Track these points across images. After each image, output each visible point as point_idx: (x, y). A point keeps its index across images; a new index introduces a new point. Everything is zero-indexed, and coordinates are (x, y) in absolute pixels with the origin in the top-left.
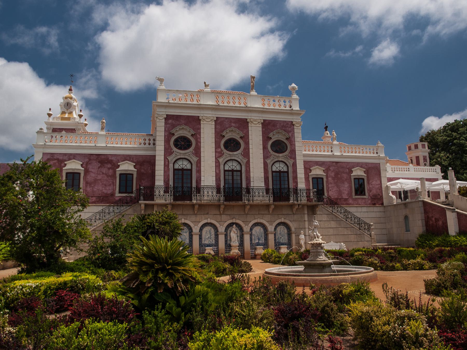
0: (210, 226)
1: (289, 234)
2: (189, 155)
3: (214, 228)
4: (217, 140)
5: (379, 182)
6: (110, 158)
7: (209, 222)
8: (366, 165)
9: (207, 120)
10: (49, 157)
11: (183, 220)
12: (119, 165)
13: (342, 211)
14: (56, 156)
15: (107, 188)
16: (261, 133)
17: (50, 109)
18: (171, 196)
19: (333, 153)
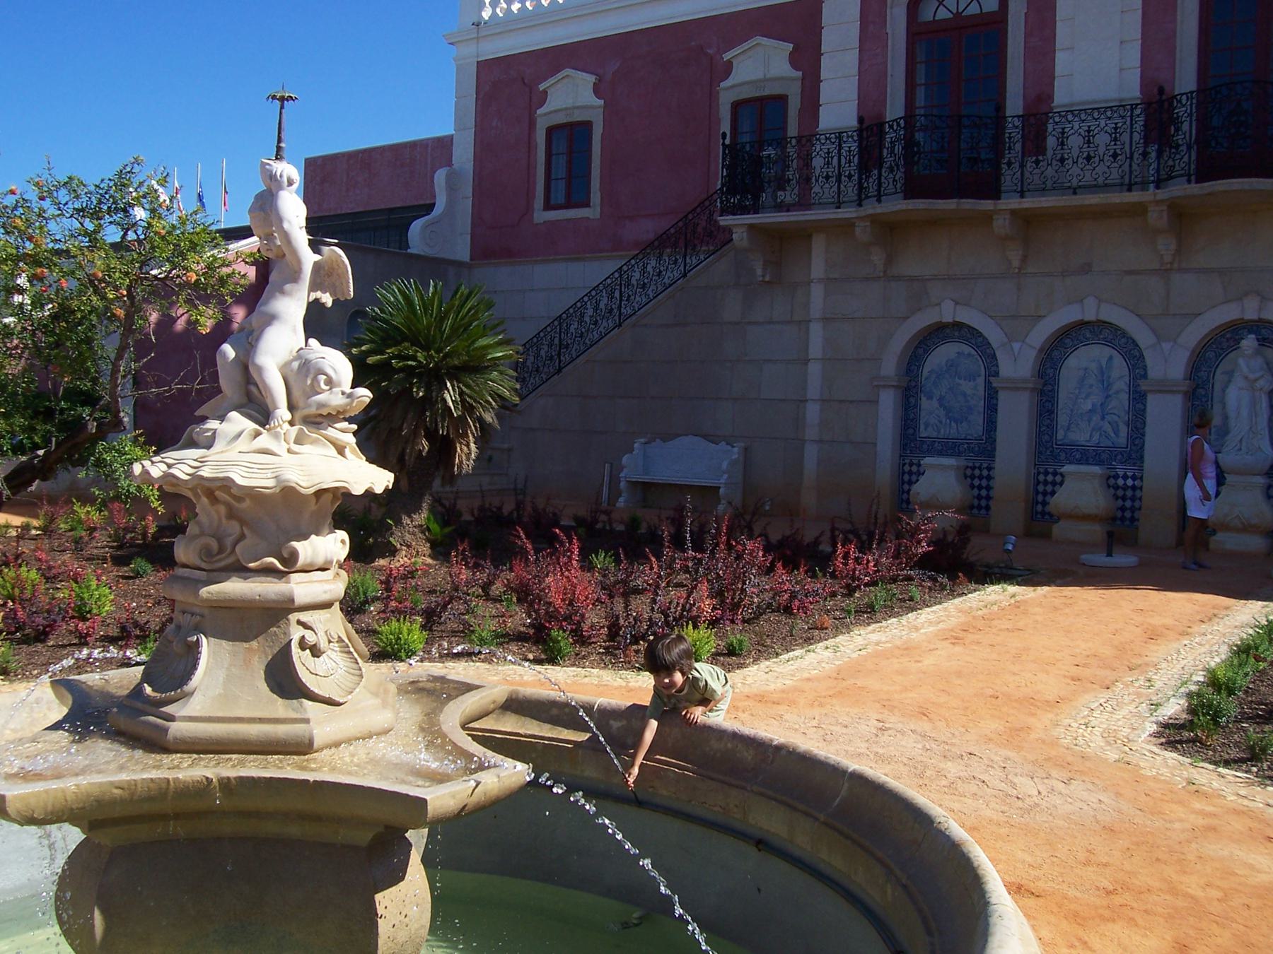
0: (1108, 343)
7: (1090, 316)
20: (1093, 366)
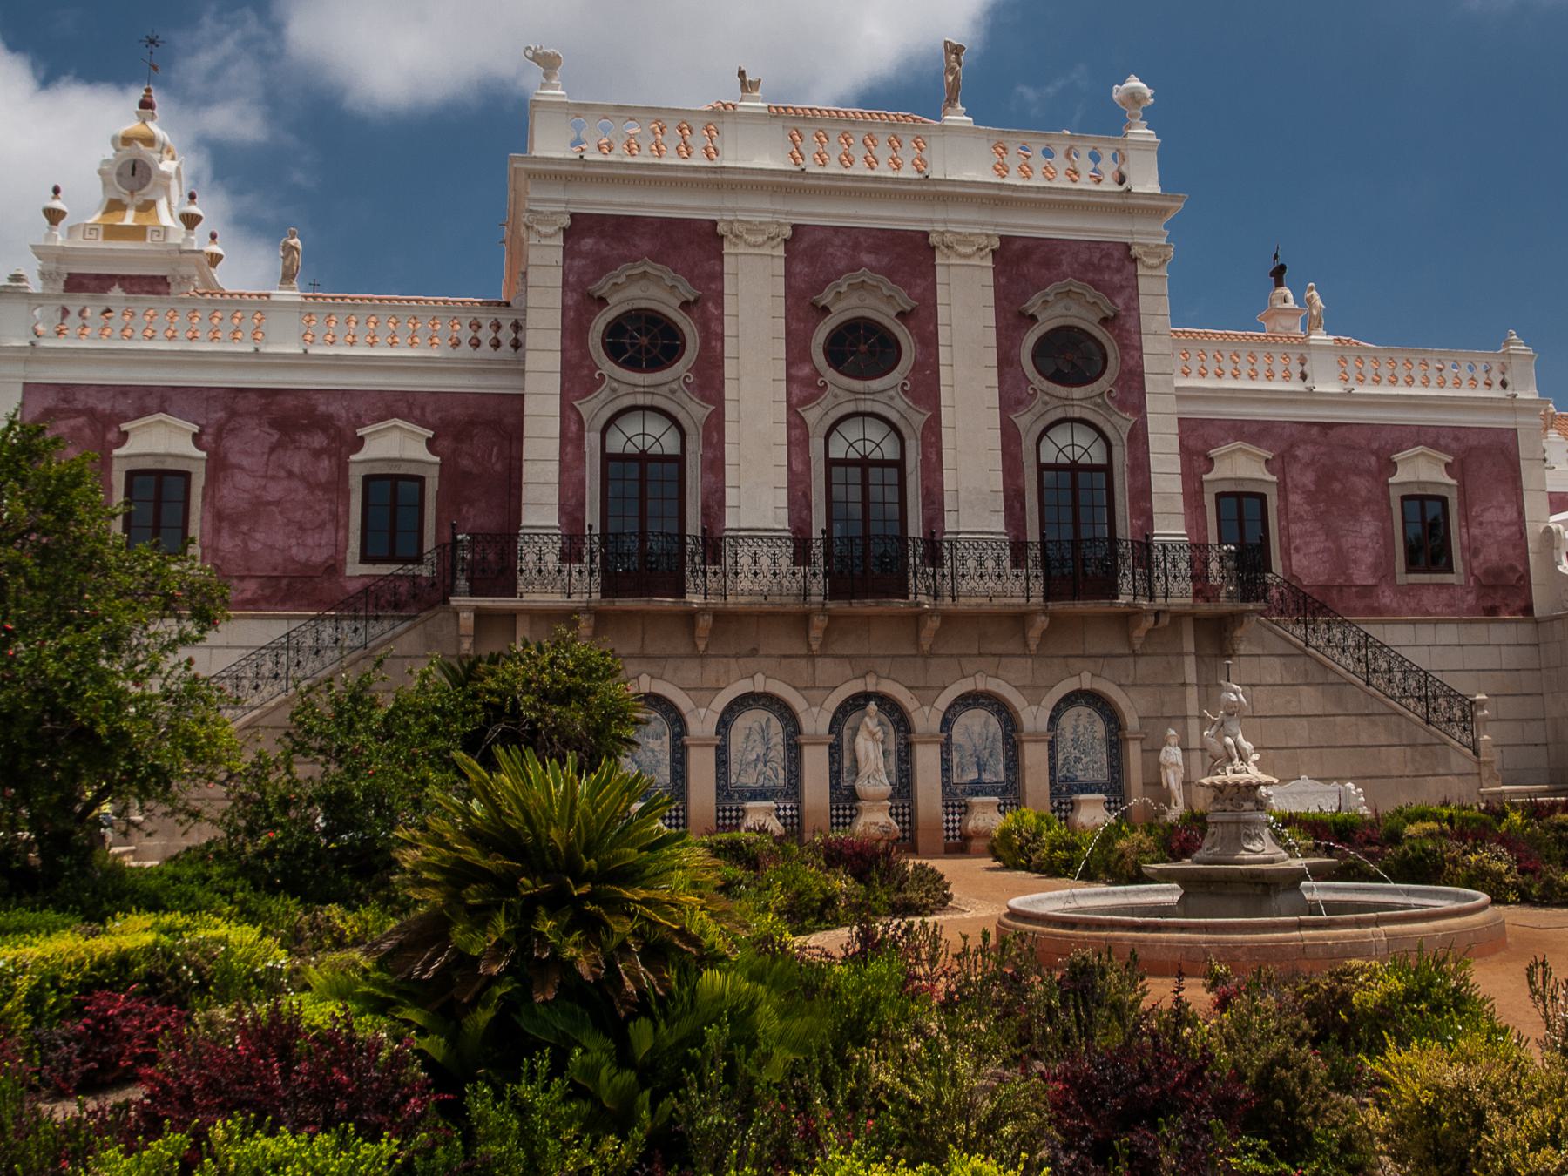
0: (765, 707)
1: (1116, 745)
2: (673, 392)
3: (781, 718)
4: (794, 325)
5: (1511, 514)
6: (322, 408)
7: (759, 689)
8: (1457, 439)
9: (752, 239)
10: (50, 401)
11: (645, 679)
12: (362, 439)
13: (1350, 642)
14: (81, 396)
15: (310, 542)
16: (990, 294)
17: (56, 190)
18: (591, 573)
19: (1308, 383)
20: (756, 725)
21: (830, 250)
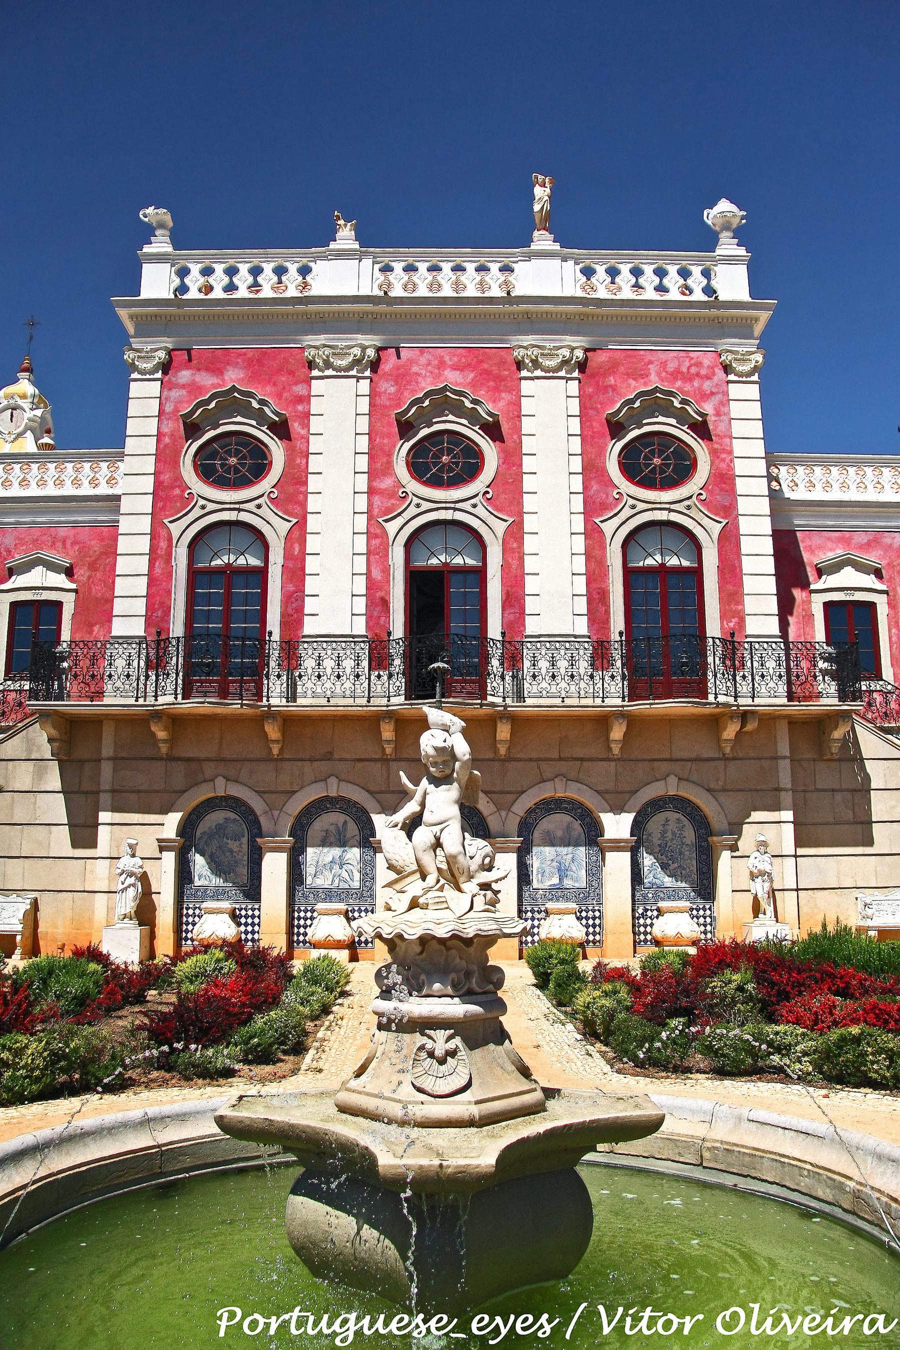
0: (343, 811)
2: (259, 507)
7: (333, 793)
11: (220, 782)
20: (332, 828)
21: (415, 369)
